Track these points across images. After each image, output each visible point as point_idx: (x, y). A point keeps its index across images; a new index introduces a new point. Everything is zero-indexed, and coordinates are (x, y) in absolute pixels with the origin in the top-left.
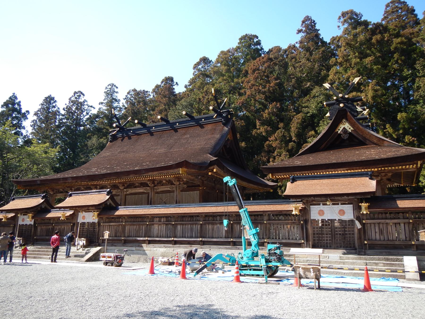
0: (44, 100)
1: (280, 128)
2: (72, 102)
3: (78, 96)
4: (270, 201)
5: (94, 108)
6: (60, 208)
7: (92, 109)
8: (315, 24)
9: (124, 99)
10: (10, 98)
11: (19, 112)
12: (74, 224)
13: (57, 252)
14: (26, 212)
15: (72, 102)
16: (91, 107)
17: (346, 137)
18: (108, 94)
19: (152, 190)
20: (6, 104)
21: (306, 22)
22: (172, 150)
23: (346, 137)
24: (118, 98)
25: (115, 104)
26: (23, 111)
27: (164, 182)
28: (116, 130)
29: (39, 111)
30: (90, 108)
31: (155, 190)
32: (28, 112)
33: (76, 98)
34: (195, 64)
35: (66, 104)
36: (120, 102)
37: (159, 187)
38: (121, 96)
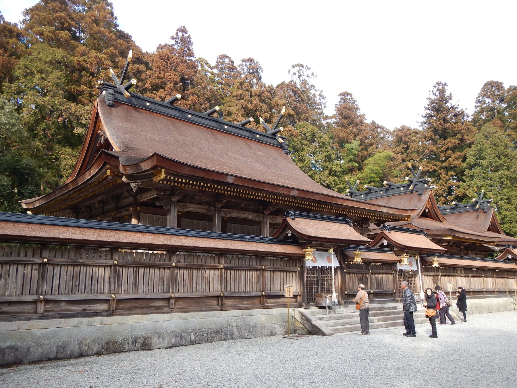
14: (321, 245)
17: (427, 211)
23: (427, 211)
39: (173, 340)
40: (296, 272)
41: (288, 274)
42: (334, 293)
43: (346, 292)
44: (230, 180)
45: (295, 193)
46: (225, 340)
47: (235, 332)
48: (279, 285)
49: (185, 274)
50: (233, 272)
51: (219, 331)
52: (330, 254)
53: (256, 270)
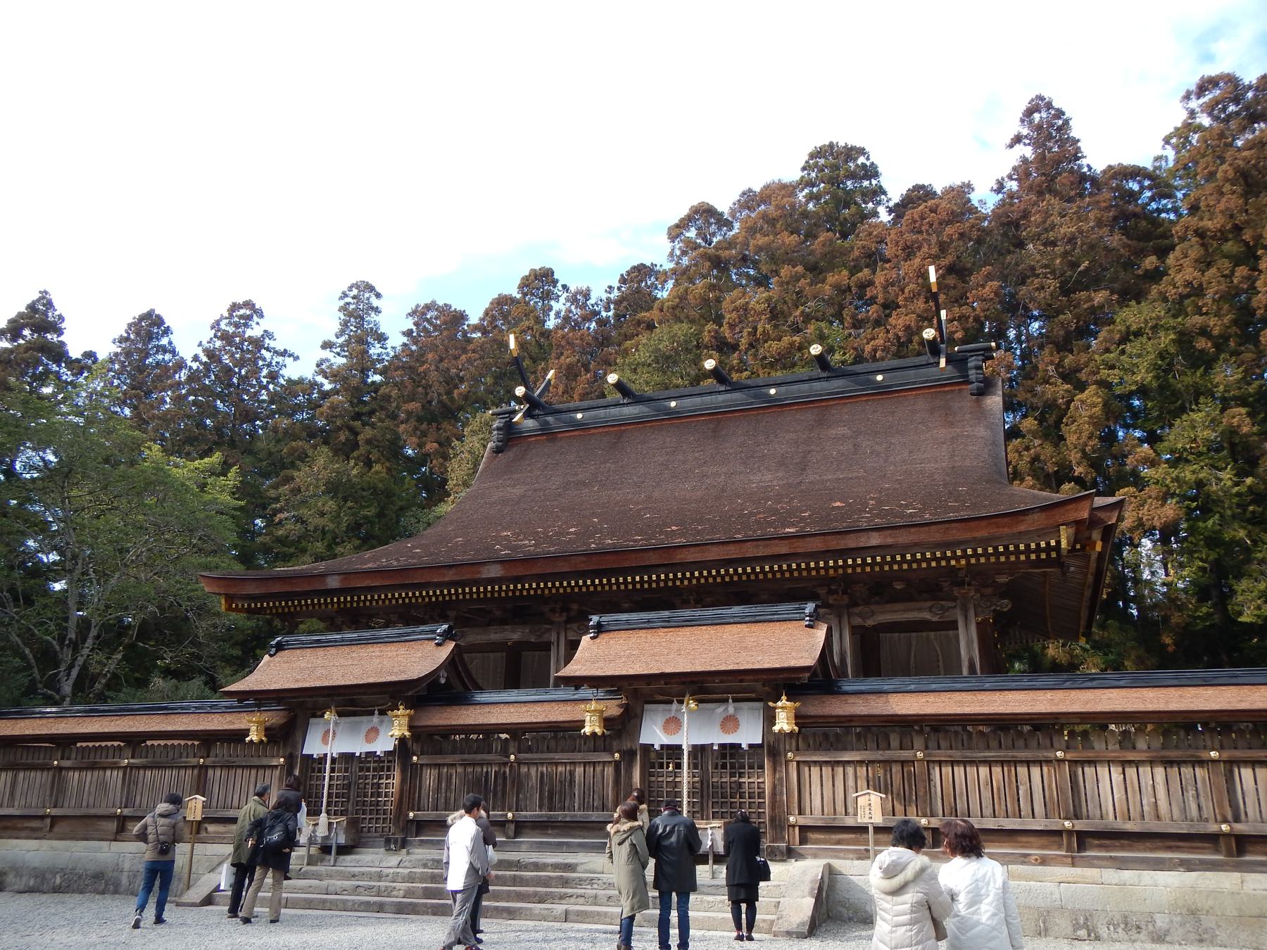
0: (130, 325)
1: (1023, 437)
2: (226, 337)
3: (241, 317)
4: (1202, 673)
5: (297, 358)
6: (576, 682)
7: (289, 361)
8: (1067, 122)
9: (404, 333)
10: (32, 307)
11: (58, 353)
12: (629, 755)
13: (752, 899)
14: (352, 703)
15: (226, 337)
16: (284, 353)
18: (350, 314)
19: (846, 618)
20: (14, 329)
21: (1037, 116)
22: (811, 477)
24: (382, 330)
25: (375, 350)
26: (75, 352)
27: (899, 586)
28: (514, 412)
29: (112, 361)
30: (280, 359)
31: (857, 621)
32: (90, 355)
33: (237, 326)
34: (677, 226)
35: (200, 344)
36: (389, 343)
37: (873, 607)
38: (394, 325)
39: (32, 882)
40: (276, 767)
41: (261, 772)
42: (324, 815)
43: (411, 814)
44: (333, 583)
45: (494, 571)
46: (103, 893)
47: (124, 881)
48: (236, 797)
49: (75, 776)
50: (148, 773)
51: (98, 876)
52: (328, 722)
53: (193, 767)
